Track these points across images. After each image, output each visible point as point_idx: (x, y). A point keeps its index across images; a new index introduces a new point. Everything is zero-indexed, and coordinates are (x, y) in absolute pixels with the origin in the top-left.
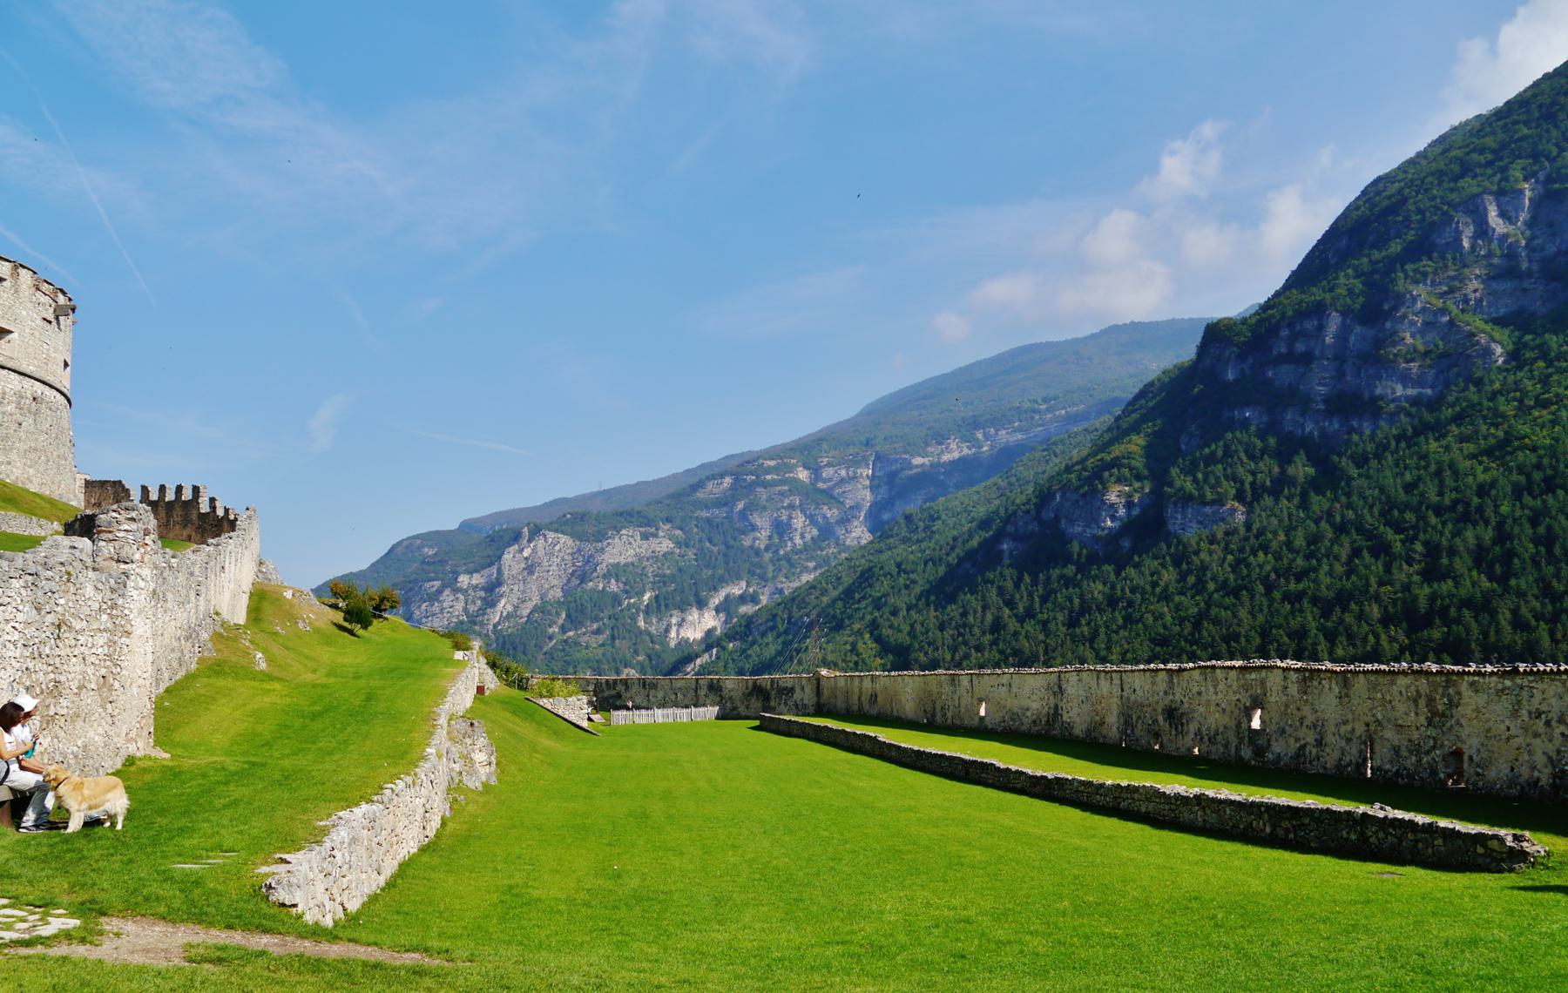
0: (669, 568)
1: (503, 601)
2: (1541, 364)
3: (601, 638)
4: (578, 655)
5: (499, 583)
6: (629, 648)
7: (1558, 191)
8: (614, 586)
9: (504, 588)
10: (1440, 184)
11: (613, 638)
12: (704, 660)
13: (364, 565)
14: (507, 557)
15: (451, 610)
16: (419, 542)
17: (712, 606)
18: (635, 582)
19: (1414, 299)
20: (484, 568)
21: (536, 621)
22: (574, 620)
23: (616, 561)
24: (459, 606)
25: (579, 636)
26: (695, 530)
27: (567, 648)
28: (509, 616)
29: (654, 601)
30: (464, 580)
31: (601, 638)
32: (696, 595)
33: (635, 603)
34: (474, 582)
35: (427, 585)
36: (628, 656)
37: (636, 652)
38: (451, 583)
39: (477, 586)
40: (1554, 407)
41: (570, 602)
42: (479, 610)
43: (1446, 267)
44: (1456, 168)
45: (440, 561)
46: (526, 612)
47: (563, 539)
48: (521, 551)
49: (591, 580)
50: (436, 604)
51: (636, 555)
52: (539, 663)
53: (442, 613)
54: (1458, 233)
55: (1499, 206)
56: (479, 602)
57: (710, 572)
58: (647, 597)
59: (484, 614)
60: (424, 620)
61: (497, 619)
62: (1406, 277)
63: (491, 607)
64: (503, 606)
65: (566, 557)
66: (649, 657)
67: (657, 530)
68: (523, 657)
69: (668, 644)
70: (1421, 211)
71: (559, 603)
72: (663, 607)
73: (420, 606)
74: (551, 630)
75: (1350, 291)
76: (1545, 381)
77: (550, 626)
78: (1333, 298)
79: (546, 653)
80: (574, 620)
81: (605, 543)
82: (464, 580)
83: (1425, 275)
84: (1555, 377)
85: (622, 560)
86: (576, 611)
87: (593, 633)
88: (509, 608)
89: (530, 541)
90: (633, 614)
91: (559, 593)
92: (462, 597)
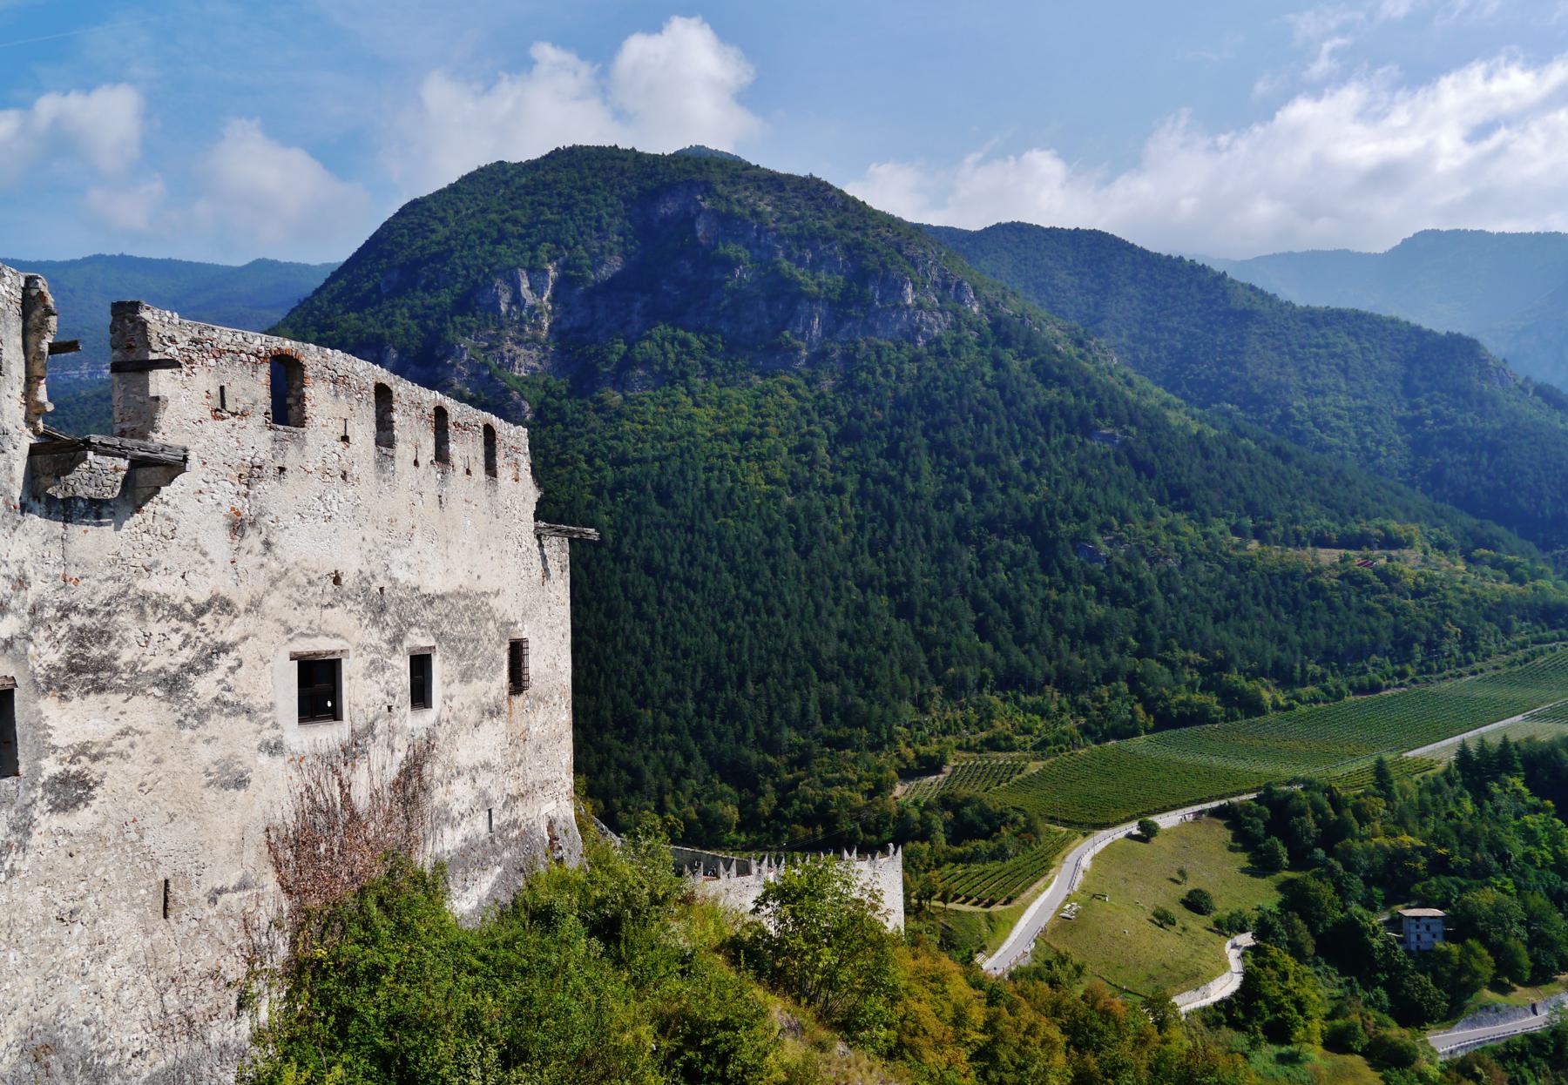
2: (559, 426)
7: (573, 277)
10: (482, 244)
19: (462, 351)
40: (570, 468)
43: (487, 324)
44: (495, 235)
54: (497, 298)
55: (529, 279)
62: (455, 328)
70: (466, 268)
75: (407, 331)
76: (563, 441)
78: (392, 336)
83: (470, 329)
84: (570, 441)
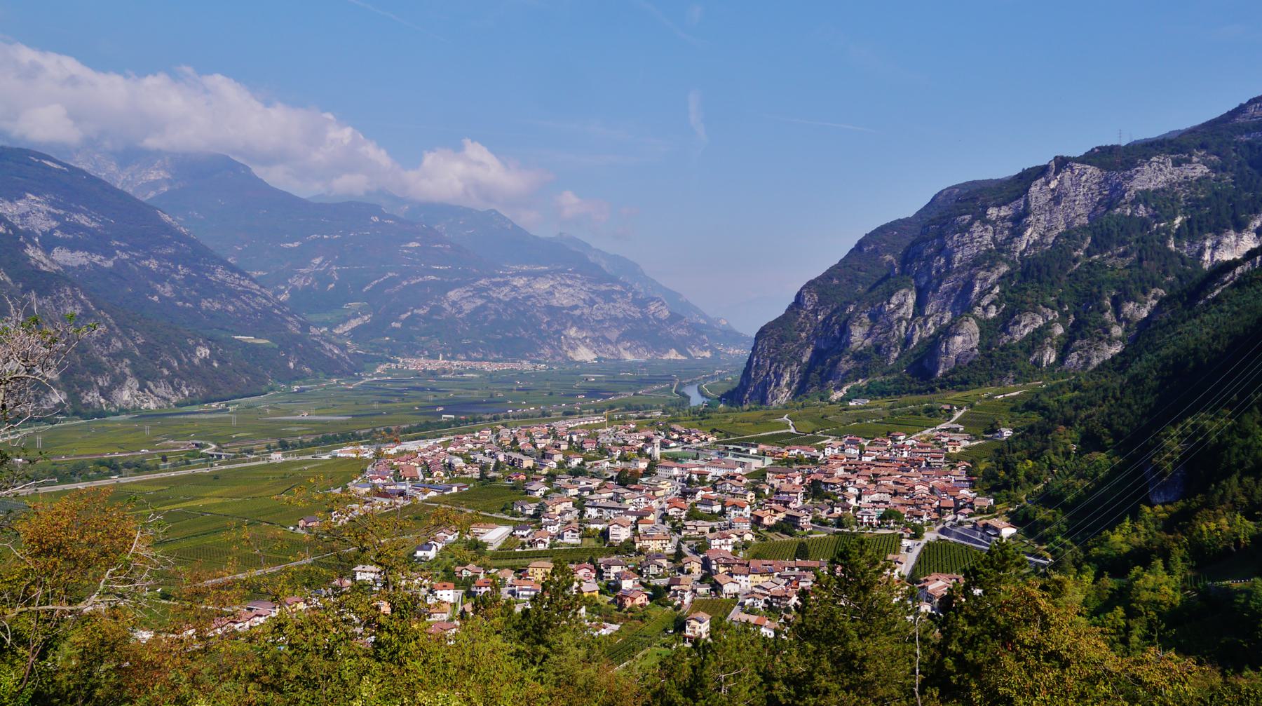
0: (1203, 192)
1: (1030, 230)
3: (1128, 261)
4: (1104, 277)
5: (1026, 213)
6: (1158, 269)
8: (1142, 211)
9: (1031, 218)
11: (1140, 260)
12: (1246, 269)
13: (911, 215)
14: (1034, 189)
15: (980, 240)
16: (957, 190)
17: (1252, 228)
18: (1165, 207)
20: (1011, 201)
21: (1061, 246)
22: (1100, 244)
23: (1145, 188)
24: (988, 237)
25: (1104, 259)
26: (1234, 154)
27: (1092, 270)
28: (1035, 244)
29: (1186, 226)
30: (993, 212)
31: (1128, 261)
32: (1234, 217)
33: (1163, 227)
34: (1002, 214)
35: (959, 219)
36: (1157, 277)
37: (1166, 273)
38: (982, 217)
39: (1005, 216)
41: (1096, 227)
42: (1006, 239)
45: (971, 198)
46: (1051, 240)
47: (1090, 169)
48: (1048, 183)
49: (1118, 207)
50: (967, 235)
51: (1167, 181)
52: (1063, 283)
53: (972, 241)
56: (1006, 232)
57: (1251, 195)
58: (1178, 221)
59: (1012, 242)
60: (956, 250)
61: (1024, 246)
63: (1018, 237)
64: (1030, 235)
65: (1093, 187)
66: (1180, 277)
67: (1191, 155)
68: (1047, 277)
69: (1201, 266)
71: (1083, 227)
72: (1196, 231)
73: (952, 238)
74: (1075, 254)
77: (1075, 250)
79: (1070, 275)
80: (1100, 244)
81: (1134, 171)
82: (993, 212)
85: (1152, 186)
86: (1102, 235)
87: (1120, 256)
88: (1036, 236)
89: (1056, 173)
90: (1162, 237)
91: (1085, 220)
92: (990, 228)
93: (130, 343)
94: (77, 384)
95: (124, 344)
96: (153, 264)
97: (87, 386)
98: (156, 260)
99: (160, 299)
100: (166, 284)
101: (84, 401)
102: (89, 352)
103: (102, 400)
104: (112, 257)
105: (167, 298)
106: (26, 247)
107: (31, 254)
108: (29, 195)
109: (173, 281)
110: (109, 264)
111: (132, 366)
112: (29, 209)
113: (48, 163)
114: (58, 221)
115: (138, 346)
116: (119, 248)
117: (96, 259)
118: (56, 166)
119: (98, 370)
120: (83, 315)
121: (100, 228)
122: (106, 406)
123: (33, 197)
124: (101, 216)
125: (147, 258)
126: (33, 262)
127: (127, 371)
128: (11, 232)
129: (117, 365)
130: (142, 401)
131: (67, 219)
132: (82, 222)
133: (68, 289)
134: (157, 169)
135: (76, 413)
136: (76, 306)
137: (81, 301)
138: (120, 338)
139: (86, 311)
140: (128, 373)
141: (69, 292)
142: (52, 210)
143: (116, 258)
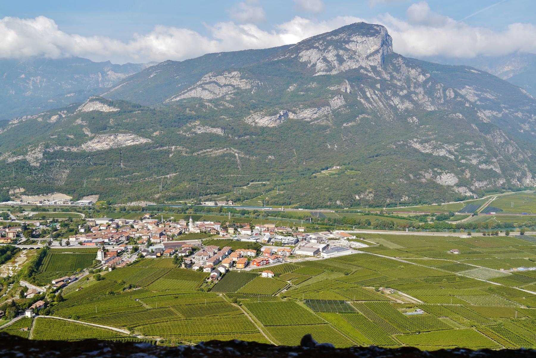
93: (526, 156)
94: (509, 175)
95: (524, 157)
96: (520, 115)
97: (513, 176)
98: (521, 112)
99: (524, 132)
100: (526, 124)
101: (512, 183)
102: (511, 161)
103: (518, 183)
104: (501, 112)
105: (527, 131)
106: (477, 112)
107: (480, 115)
108: (467, 86)
109: (529, 122)
110: (500, 115)
111: (528, 167)
112: (466, 93)
113: (473, 71)
114: (478, 97)
115: (529, 157)
116: (504, 107)
117: (495, 113)
118: (476, 72)
119: (517, 169)
120: (505, 143)
121: (496, 99)
122: (520, 185)
123: (468, 87)
124: (496, 93)
125: (517, 112)
126: (481, 119)
127: (526, 169)
128: (471, 106)
129: (521, 166)
130: (533, 183)
131: (482, 96)
132: (488, 96)
133: (498, 131)
134: (508, 65)
135: (509, 189)
136: (502, 139)
137: (504, 137)
138: (522, 153)
139: (506, 140)
140: (527, 170)
141: (498, 132)
142: (476, 92)
143: (503, 112)
